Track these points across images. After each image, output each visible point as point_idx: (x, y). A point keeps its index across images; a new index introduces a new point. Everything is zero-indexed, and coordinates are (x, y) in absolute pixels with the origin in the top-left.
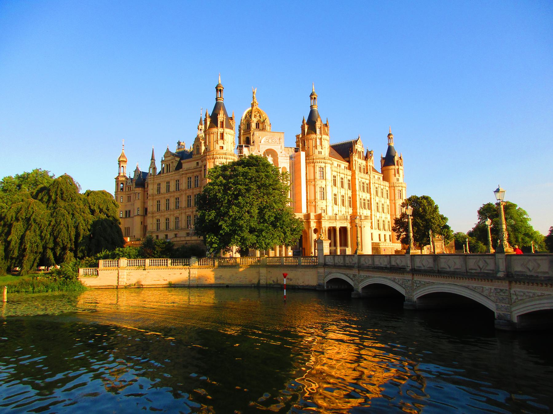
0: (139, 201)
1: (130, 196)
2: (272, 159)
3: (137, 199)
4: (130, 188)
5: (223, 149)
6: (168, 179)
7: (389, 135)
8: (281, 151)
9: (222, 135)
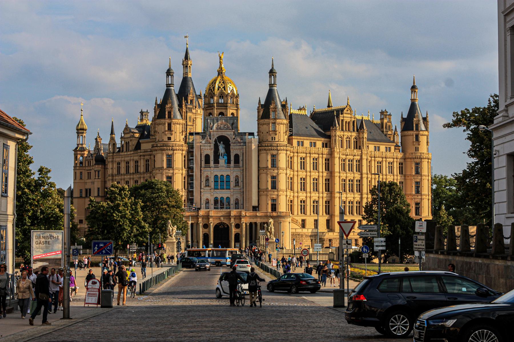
0: (98, 180)
1: (90, 172)
2: (224, 146)
3: (97, 177)
4: (89, 163)
5: (170, 140)
6: (127, 159)
7: (414, 88)
8: (234, 137)
9: (170, 125)
